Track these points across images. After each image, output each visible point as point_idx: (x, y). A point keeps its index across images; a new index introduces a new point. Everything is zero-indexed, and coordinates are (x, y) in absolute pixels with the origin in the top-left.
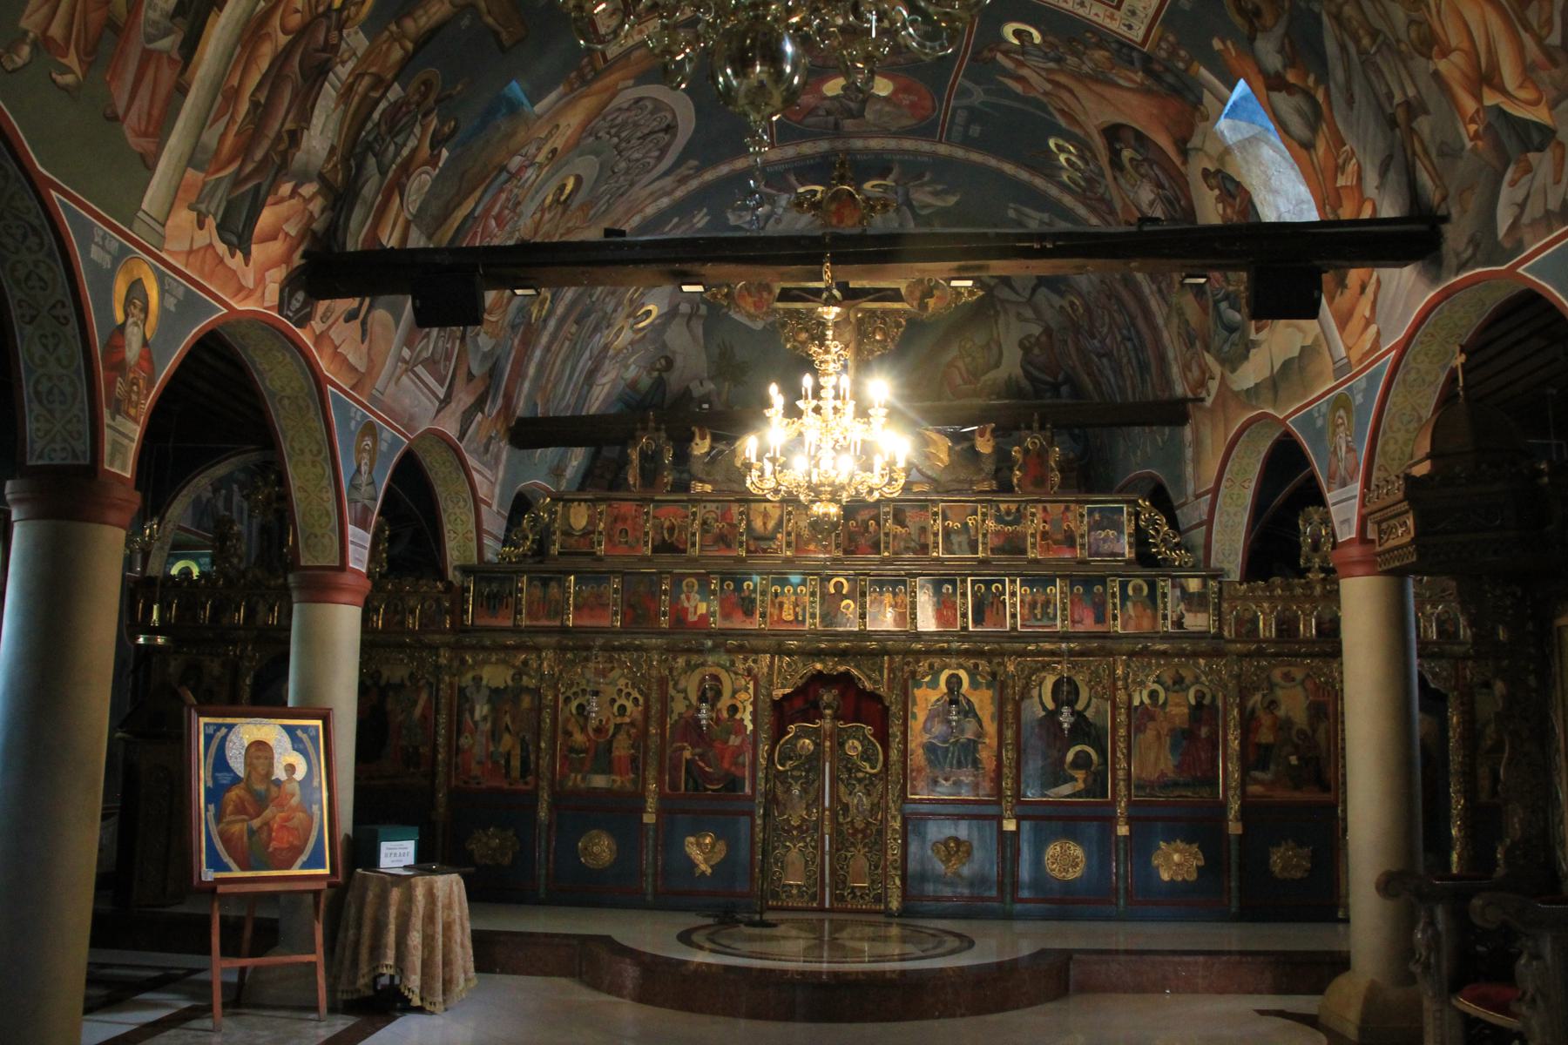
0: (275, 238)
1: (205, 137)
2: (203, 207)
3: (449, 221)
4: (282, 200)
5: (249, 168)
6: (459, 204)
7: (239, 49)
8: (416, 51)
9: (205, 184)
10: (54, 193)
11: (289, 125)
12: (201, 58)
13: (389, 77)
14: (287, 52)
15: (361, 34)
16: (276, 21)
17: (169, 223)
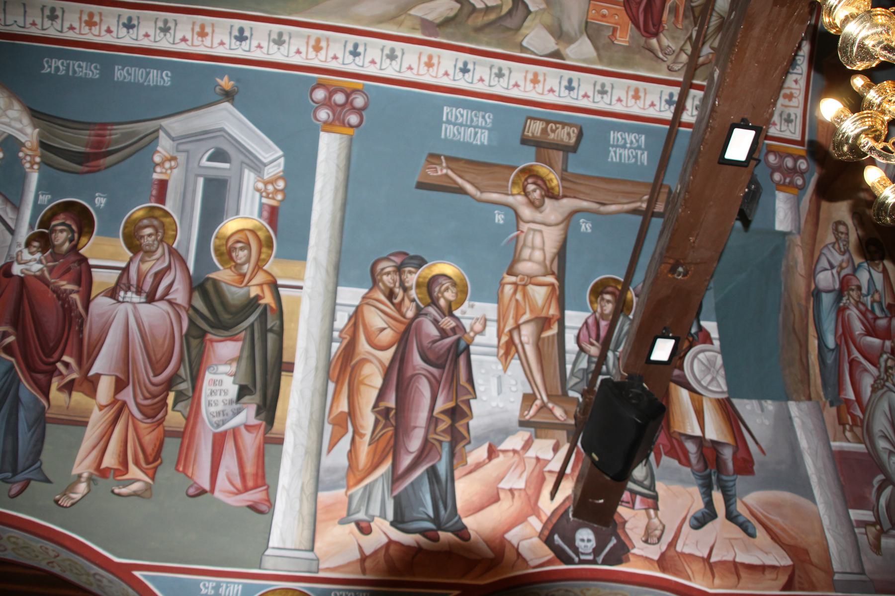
0: (496, 499)
1: (327, 461)
2: (361, 516)
3: (811, 372)
4: (478, 466)
5: (406, 461)
6: (807, 352)
7: (331, 386)
8: (561, 276)
9: (350, 498)
10: (137, 574)
11: (440, 405)
12: (285, 410)
13: (553, 311)
14: (401, 359)
15: (477, 304)
16: (363, 346)
17: (318, 545)
